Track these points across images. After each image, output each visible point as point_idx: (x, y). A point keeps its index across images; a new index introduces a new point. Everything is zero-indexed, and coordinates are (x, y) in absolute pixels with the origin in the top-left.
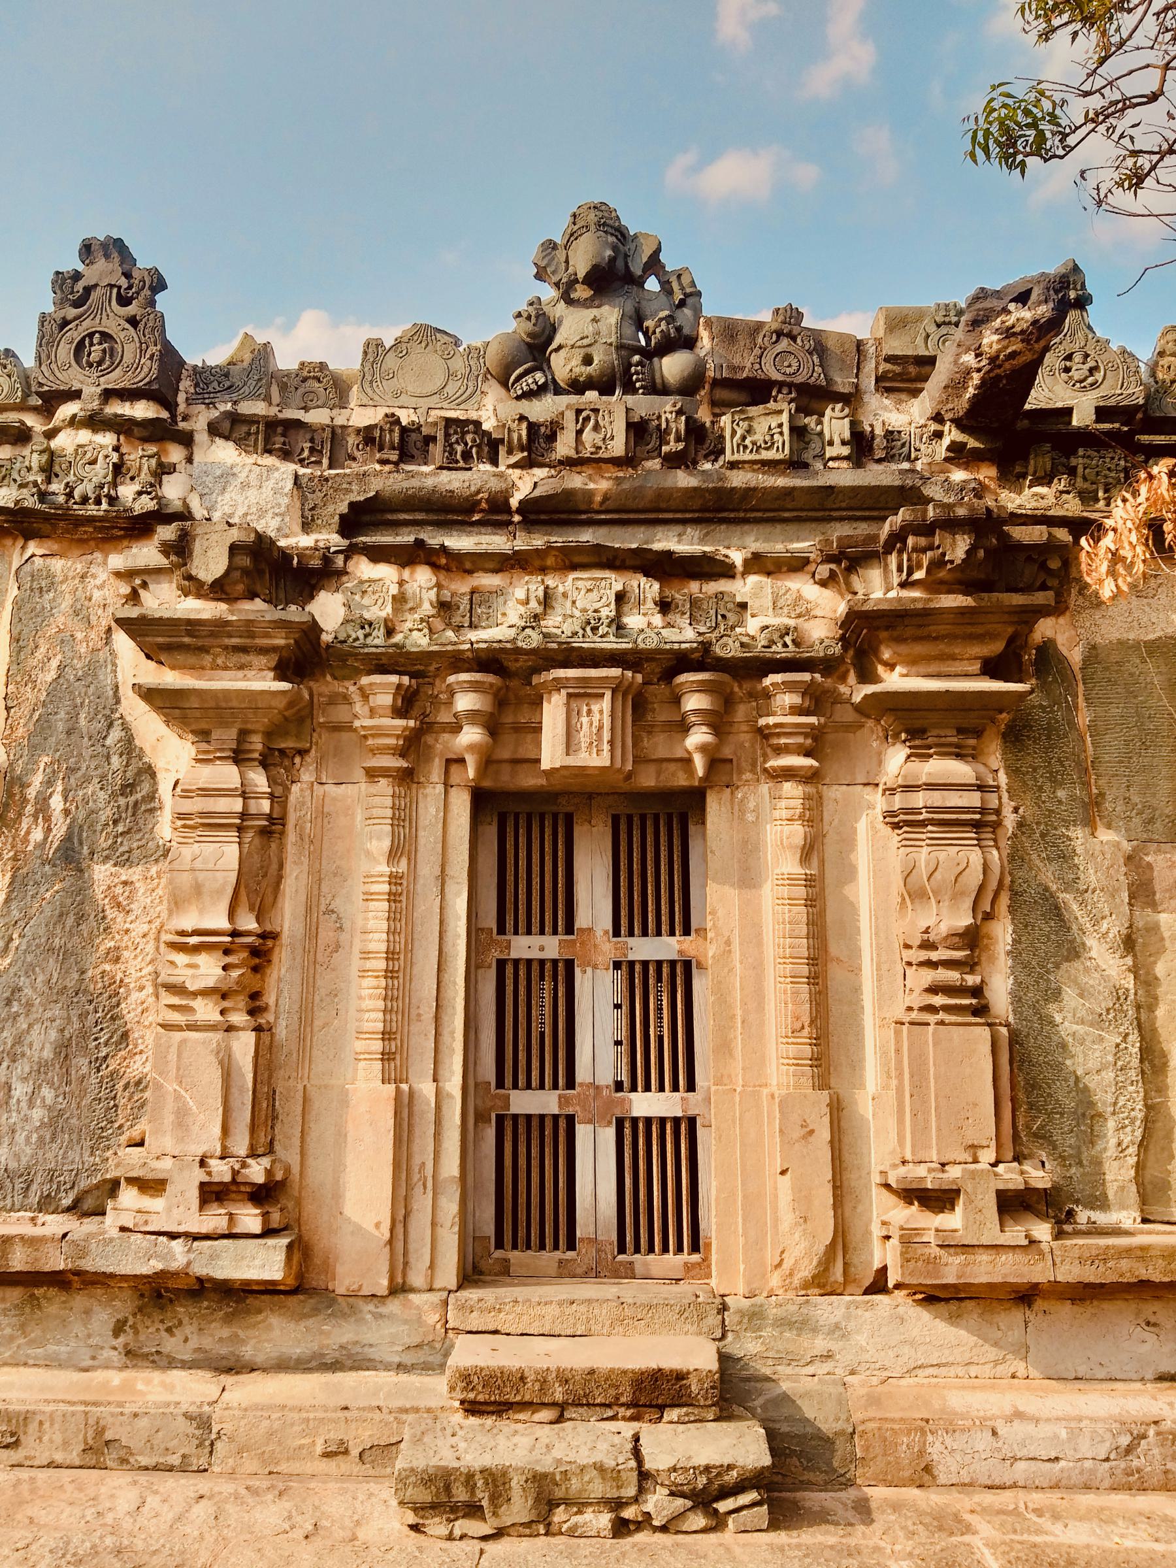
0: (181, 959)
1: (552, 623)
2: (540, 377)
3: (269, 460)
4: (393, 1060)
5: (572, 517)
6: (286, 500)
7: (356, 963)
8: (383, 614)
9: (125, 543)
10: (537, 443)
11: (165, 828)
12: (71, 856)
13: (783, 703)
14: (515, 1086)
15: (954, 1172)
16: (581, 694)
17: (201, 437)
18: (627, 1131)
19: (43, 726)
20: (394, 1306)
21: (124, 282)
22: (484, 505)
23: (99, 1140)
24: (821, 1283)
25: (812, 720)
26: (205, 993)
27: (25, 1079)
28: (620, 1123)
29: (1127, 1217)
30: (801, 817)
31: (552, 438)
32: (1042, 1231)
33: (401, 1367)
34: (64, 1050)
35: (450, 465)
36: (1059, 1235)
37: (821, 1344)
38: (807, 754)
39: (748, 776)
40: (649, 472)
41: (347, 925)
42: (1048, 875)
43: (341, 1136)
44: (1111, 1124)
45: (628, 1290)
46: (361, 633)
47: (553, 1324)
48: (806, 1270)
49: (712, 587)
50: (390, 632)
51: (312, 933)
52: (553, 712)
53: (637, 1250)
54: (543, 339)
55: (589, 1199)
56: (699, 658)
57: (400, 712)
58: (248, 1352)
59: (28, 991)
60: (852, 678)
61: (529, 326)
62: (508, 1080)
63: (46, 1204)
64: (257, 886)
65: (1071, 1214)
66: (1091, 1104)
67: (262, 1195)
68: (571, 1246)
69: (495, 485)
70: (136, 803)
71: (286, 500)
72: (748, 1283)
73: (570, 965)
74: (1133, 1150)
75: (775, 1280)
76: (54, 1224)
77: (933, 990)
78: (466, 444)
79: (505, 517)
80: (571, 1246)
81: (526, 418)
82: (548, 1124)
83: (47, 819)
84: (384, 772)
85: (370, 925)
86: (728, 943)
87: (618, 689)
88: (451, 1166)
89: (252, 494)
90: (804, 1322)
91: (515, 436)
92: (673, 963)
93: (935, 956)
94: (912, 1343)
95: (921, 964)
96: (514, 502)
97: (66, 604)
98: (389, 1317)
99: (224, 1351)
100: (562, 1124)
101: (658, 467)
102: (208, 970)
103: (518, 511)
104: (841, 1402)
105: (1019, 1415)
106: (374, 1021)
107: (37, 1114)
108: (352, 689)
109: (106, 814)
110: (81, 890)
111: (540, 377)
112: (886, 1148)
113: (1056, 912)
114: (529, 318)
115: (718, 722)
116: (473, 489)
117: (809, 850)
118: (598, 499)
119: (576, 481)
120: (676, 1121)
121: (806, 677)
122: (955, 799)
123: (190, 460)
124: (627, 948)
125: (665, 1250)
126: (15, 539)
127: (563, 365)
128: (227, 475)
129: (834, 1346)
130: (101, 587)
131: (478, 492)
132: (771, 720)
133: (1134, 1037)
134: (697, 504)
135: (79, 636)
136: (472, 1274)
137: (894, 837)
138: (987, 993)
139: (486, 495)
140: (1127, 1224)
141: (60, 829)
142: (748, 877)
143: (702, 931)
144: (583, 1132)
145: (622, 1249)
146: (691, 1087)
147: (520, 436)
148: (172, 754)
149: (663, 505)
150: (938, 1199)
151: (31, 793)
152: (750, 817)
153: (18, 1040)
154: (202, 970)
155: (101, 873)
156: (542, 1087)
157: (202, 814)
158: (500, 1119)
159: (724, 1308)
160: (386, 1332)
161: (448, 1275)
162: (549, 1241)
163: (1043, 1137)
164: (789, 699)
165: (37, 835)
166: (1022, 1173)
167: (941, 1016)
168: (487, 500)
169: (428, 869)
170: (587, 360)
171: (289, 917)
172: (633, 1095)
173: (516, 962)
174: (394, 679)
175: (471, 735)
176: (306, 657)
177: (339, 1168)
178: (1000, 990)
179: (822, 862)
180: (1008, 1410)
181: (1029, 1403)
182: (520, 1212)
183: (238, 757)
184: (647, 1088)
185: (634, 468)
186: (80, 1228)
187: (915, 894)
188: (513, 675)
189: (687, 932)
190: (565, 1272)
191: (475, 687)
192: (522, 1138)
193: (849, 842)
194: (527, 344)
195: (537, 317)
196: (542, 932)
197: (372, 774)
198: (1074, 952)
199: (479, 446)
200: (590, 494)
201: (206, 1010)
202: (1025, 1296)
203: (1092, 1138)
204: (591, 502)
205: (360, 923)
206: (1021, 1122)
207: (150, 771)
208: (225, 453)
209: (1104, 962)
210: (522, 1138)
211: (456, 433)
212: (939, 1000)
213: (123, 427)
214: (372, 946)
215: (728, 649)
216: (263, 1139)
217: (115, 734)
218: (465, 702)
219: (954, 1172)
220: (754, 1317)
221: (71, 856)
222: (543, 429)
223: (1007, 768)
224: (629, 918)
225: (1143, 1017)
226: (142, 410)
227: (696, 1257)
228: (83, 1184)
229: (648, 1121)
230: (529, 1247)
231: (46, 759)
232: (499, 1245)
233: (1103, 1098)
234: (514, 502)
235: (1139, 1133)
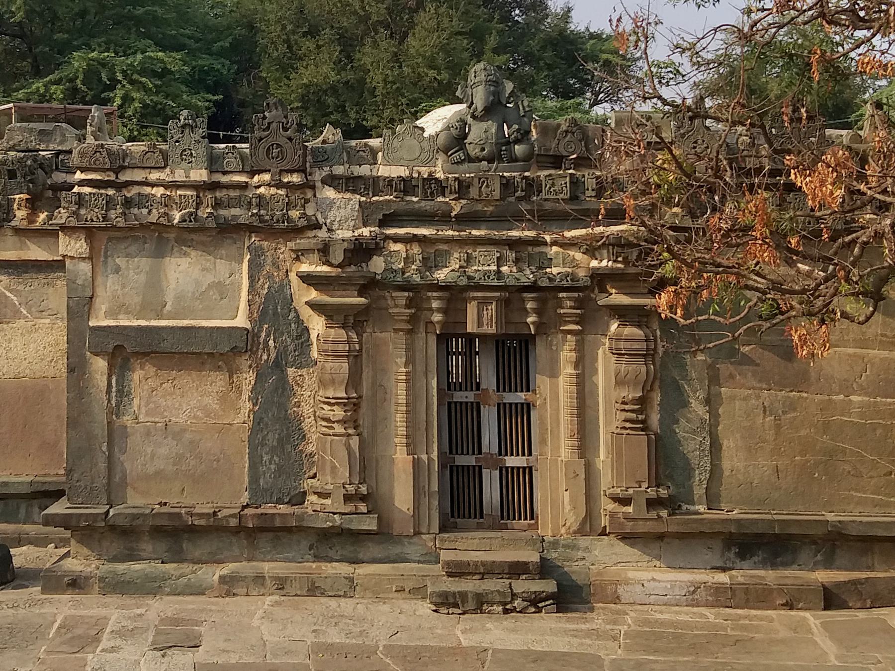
0: (326, 407)
1: (471, 270)
3: (348, 195)
4: (411, 447)
6: (356, 214)
7: (393, 408)
8: (400, 266)
9: (292, 235)
10: (462, 189)
11: (315, 354)
12: (279, 365)
13: (567, 308)
14: (457, 453)
15: (631, 491)
16: (483, 303)
17: (319, 184)
18: (504, 472)
19: (263, 314)
20: (415, 539)
21: (284, 120)
23: (298, 476)
24: (581, 531)
25: (579, 311)
26: (338, 422)
27: (267, 454)
28: (501, 469)
29: (702, 508)
30: (575, 350)
32: (664, 513)
33: (419, 562)
34: (280, 440)
35: (425, 198)
36: (670, 515)
37: (580, 554)
38: (577, 323)
39: (553, 330)
41: (388, 391)
42: (675, 374)
43: (392, 475)
44: (697, 472)
45: (505, 534)
46: (392, 275)
47: (474, 546)
48: (575, 528)
49: (538, 249)
50: (403, 273)
51: (374, 394)
52: (472, 309)
53: (509, 519)
55: (489, 499)
56: (533, 288)
57: (407, 306)
58: (361, 556)
59: (266, 419)
60: (596, 291)
62: (454, 452)
63: (279, 501)
64: (354, 380)
65: (680, 506)
66: (690, 465)
67: (363, 498)
68: (482, 517)
69: (444, 207)
70: (302, 343)
71: (356, 214)
72: (552, 531)
73: (478, 404)
74: (705, 482)
75: (563, 531)
76: (283, 509)
77: (626, 421)
80: (482, 517)
82: (471, 468)
83: (268, 350)
84: (401, 330)
85: (401, 392)
86: (545, 399)
87: (498, 300)
88: (435, 487)
89: (342, 210)
90: (574, 546)
92: (522, 404)
93: (627, 407)
94: (616, 554)
95: (622, 410)
97: (269, 261)
98: (414, 543)
99: (352, 555)
100: (477, 468)
102: (339, 413)
104: (587, 574)
105: (654, 579)
106: (402, 431)
107: (273, 467)
108: (387, 294)
109: (291, 348)
110: (283, 378)
112: (606, 481)
113: (679, 389)
115: (538, 312)
117: (577, 365)
120: (524, 468)
121: (576, 295)
122: (636, 346)
123: (315, 196)
124: (502, 398)
125: (520, 519)
126: (245, 231)
128: (332, 202)
129: (585, 555)
130: (283, 253)
132: (562, 311)
133: (708, 438)
135: (275, 274)
136: (443, 529)
137: (614, 358)
138: (649, 422)
140: (702, 510)
141: (273, 356)
142: (554, 374)
143: (534, 391)
144: (485, 472)
145: (502, 519)
146: (530, 454)
148: (317, 325)
150: (625, 501)
151: (261, 340)
152: (554, 348)
153: (264, 438)
154: (336, 413)
155: (291, 371)
156: (468, 454)
157: (333, 351)
158: (451, 467)
159: (544, 540)
160: (412, 549)
161: (436, 528)
162: (473, 516)
163: (670, 477)
164: (569, 303)
165: (265, 357)
166: (657, 491)
167: (628, 431)
169: (420, 368)
171: (365, 390)
172: (506, 458)
173: (456, 403)
174: (406, 294)
175: (437, 317)
176: (369, 285)
177: (392, 488)
178: (655, 419)
179: (583, 367)
180: (650, 578)
181: (658, 575)
182: (459, 502)
183: (344, 327)
184: (512, 455)
186: (296, 509)
187: (620, 382)
188: (455, 295)
189: (528, 390)
190: (480, 527)
191: (439, 298)
192: (460, 474)
193: (596, 359)
196: (466, 390)
197: (396, 331)
198: (685, 404)
201: (339, 429)
202: (660, 537)
203: (690, 477)
205: (394, 391)
206: (661, 471)
207: (307, 329)
208: (330, 193)
209: (698, 408)
210: (460, 474)
212: (628, 425)
213: (289, 186)
214: (400, 401)
215: (544, 283)
216: (362, 477)
217: (292, 314)
218: (435, 305)
219: (631, 491)
220: (555, 544)
221: (279, 365)
223: (660, 328)
224: (505, 383)
225: (713, 430)
226: (296, 178)
227: (533, 522)
228: (292, 494)
229: (513, 468)
230: (464, 517)
231: (266, 326)
232: (453, 516)
233: (695, 462)
235: (708, 476)
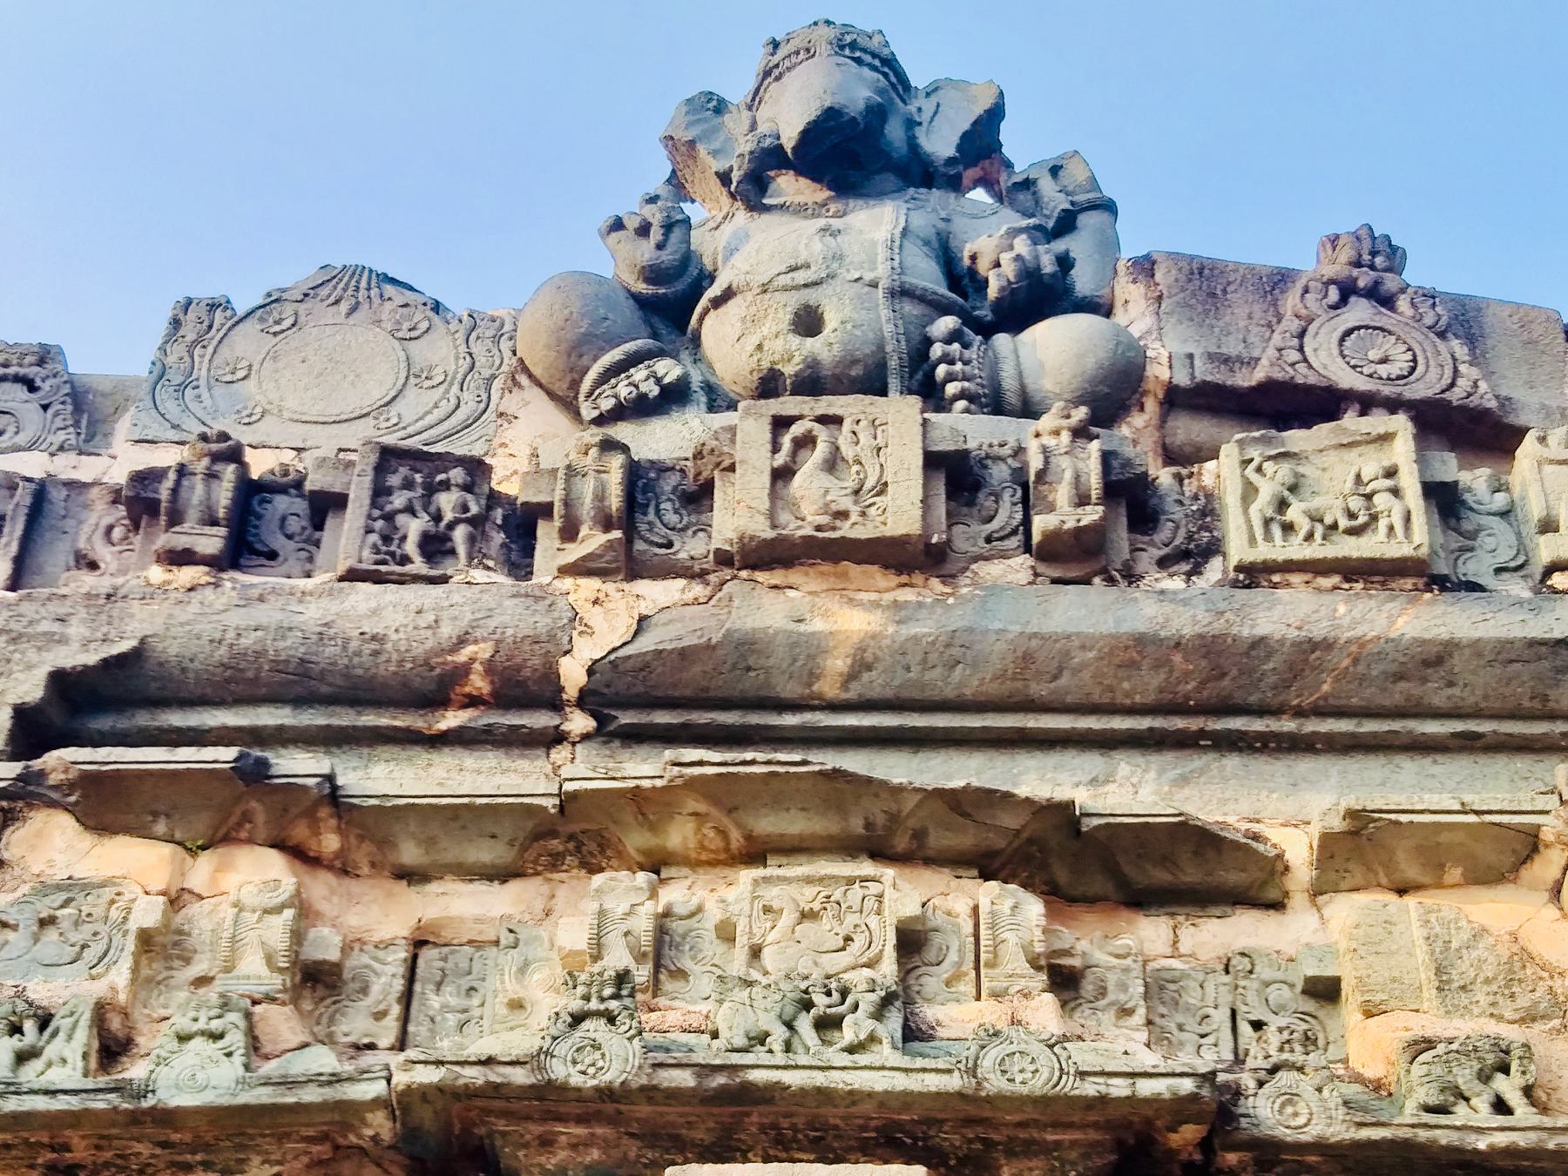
2: (669, 370)
5: (755, 719)
22: (478, 683)
31: (698, 497)
40: (994, 590)
54: (680, 286)
61: (645, 251)
78: (437, 518)
79: (540, 720)
81: (624, 449)
91: (586, 490)
96: (573, 674)
101: (1025, 576)
103: (585, 700)
111: (669, 370)
114: (644, 230)
116: (448, 631)
118: (838, 664)
119: (768, 609)
127: (732, 341)
131: (462, 641)
134: (1148, 685)
139: (484, 651)
147: (600, 497)
149: (1039, 690)
168: (490, 668)
170: (808, 323)
185: (948, 578)
194: (637, 298)
195: (668, 227)
199: (477, 522)
200: (809, 651)
204: (813, 676)
211: (408, 485)
222: (669, 482)
234: (573, 674)
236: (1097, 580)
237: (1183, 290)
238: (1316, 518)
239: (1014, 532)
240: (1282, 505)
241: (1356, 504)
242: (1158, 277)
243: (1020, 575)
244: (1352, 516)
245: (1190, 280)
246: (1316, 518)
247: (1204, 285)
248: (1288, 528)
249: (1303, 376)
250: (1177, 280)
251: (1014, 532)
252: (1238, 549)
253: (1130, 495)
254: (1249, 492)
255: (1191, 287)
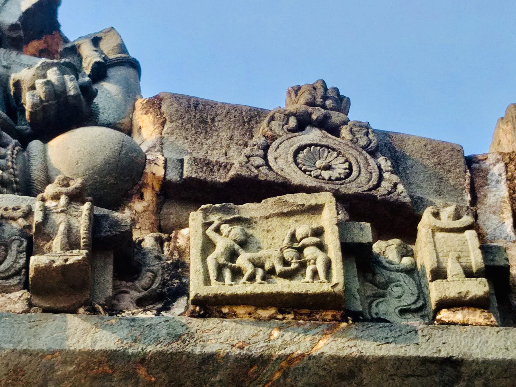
101: (20, 306)
236: (81, 310)
237: (181, 117)
238: (258, 264)
239: (17, 273)
240: (233, 255)
241: (289, 254)
242: (163, 108)
243: (17, 306)
244: (286, 263)
245: (187, 111)
246: (258, 264)
247: (197, 115)
248: (237, 273)
249: (264, 174)
250: (177, 111)
251: (17, 273)
252: (196, 287)
253: (112, 247)
254: (208, 246)
255: (187, 116)
